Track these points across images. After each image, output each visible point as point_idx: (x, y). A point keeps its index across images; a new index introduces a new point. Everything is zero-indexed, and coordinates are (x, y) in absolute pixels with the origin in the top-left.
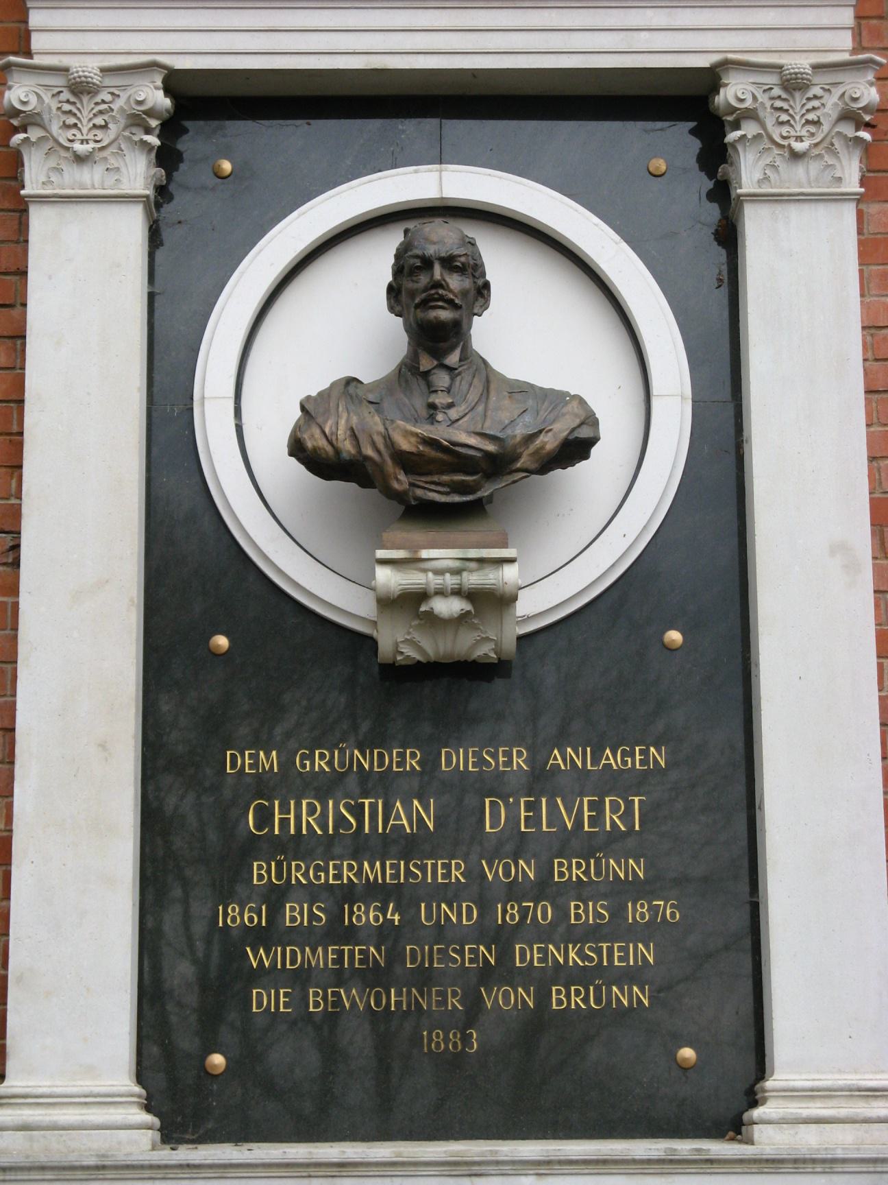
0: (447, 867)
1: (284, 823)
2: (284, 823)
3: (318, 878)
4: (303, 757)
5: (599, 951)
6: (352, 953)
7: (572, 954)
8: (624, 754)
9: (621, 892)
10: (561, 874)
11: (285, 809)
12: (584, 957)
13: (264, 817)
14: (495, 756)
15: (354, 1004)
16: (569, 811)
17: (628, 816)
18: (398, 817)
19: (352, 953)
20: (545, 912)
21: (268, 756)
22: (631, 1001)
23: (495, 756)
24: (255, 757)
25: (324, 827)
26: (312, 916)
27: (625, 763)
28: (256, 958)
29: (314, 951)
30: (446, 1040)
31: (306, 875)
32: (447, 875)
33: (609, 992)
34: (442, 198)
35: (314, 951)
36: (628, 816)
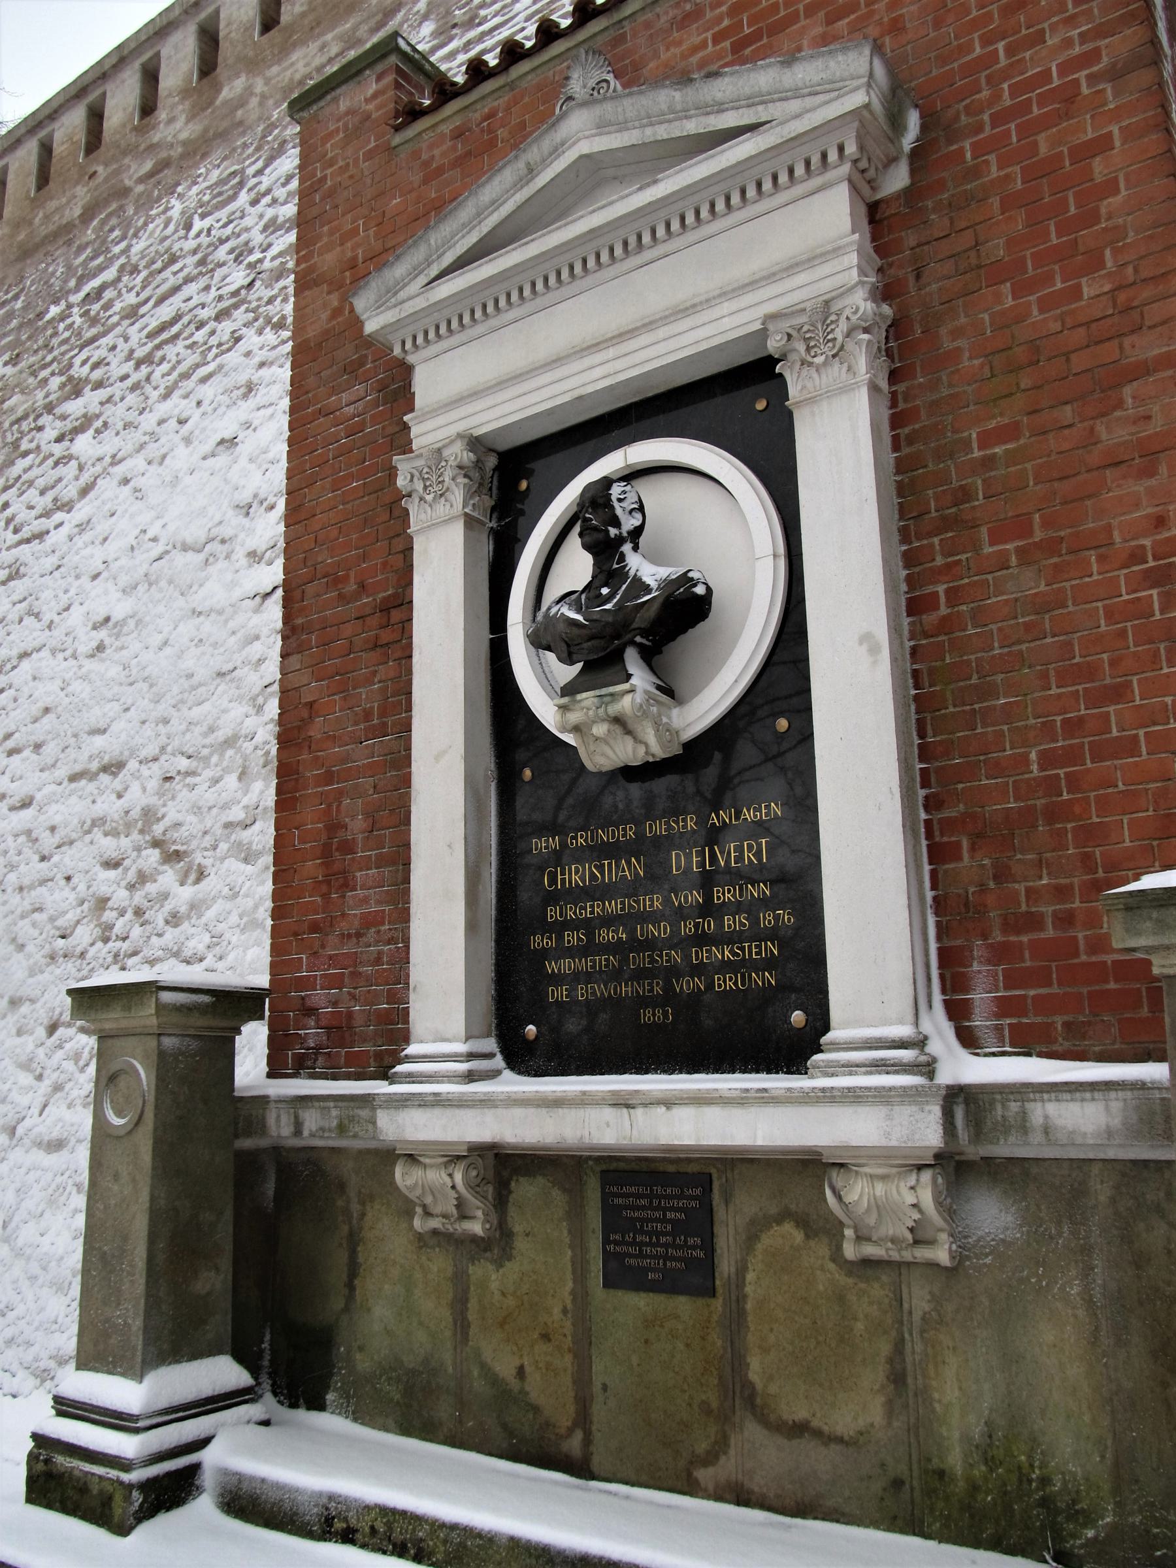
0: (651, 900)
1: (563, 880)
2: (563, 880)
3: (581, 914)
4: (572, 838)
5: (742, 949)
6: (600, 960)
7: (726, 953)
8: (755, 810)
9: (750, 909)
10: (719, 898)
11: (563, 874)
12: (734, 954)
13: (553, 880)
14: (677, 823)
15: (602, 994)
16: (722, 853)
17: (758, 854)
18: (623, 871)
19: (600, 960)
20: (710, 926)
21: (554, 840)
22: (763, 983)
23: (677, 823)
24: (547, 841)
25: (584, 881)
26: (579, 939)
27: (755, 816)
28: (551, 967)
29: (580, 961)
30: (654, 1015)
31: (575, 913)
32: (651, 906)
33: (750, 976)
34: (628, 466)
35: (580, 961)
36: (758, 854)
